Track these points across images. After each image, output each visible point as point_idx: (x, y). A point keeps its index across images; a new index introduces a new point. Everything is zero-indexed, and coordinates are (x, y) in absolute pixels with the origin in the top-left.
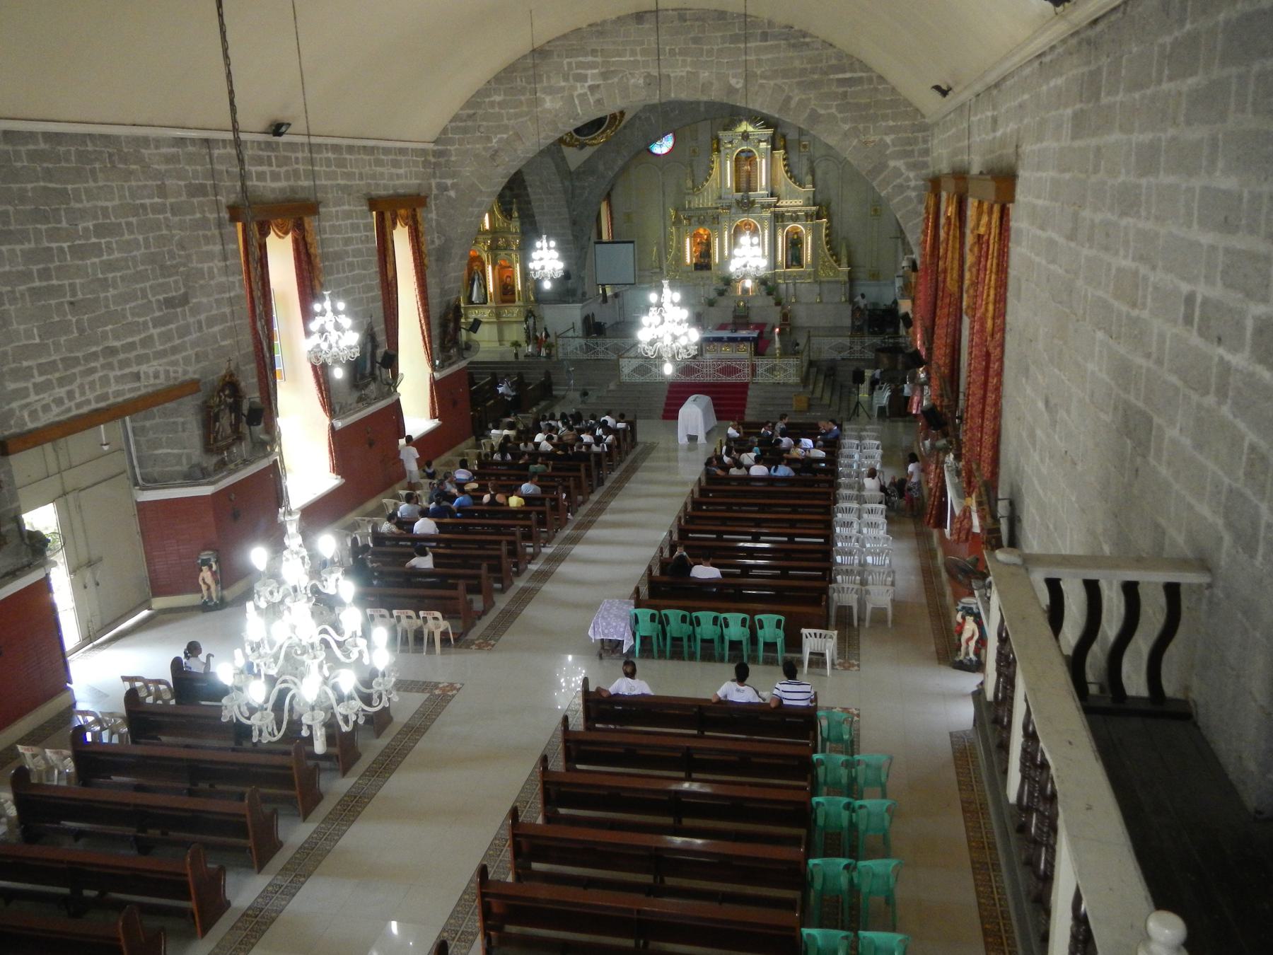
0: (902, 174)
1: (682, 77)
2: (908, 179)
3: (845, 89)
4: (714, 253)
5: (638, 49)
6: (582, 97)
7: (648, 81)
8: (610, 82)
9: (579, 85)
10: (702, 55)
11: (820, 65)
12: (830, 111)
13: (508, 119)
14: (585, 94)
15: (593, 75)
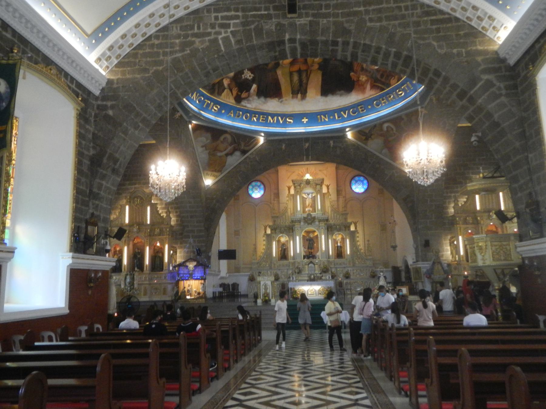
0: (495, 85)
1: (305, 24)
2: (499, 89)
3: (438, 26)
4: (290, 250)
5: (271, 6)
6: (226, 40)
7: (278, 28)
8: (248, 28)
9: (223, 31)
10: (321, 9)
11: (415, 12)
12: (427, 41)
13: (163, 56)
14: (229, 36)
15: (234, 24)
